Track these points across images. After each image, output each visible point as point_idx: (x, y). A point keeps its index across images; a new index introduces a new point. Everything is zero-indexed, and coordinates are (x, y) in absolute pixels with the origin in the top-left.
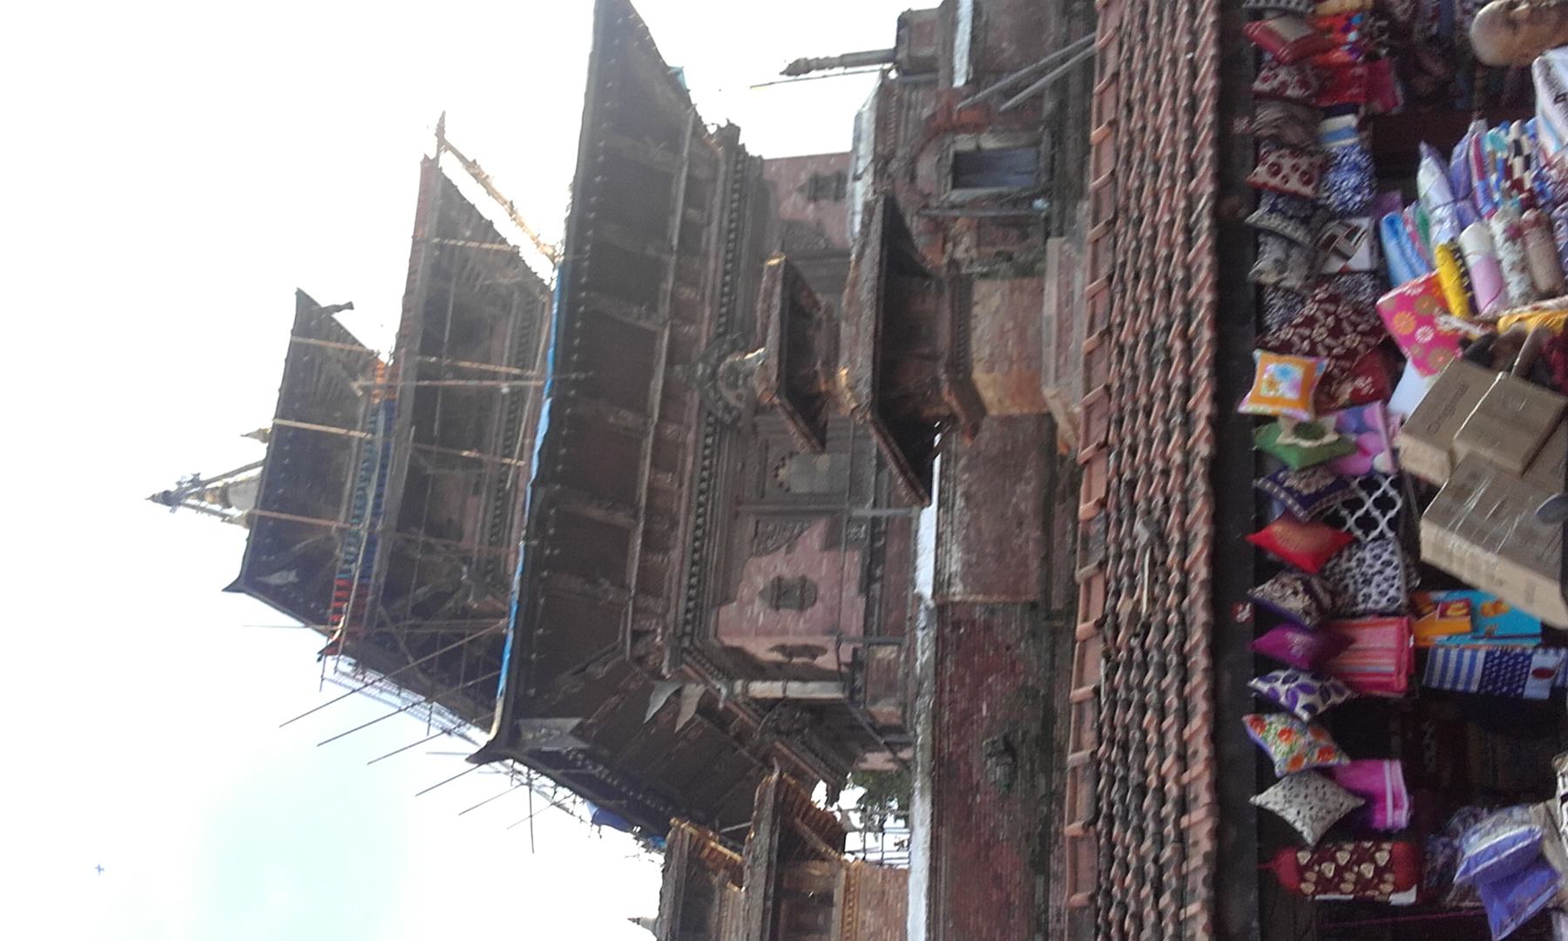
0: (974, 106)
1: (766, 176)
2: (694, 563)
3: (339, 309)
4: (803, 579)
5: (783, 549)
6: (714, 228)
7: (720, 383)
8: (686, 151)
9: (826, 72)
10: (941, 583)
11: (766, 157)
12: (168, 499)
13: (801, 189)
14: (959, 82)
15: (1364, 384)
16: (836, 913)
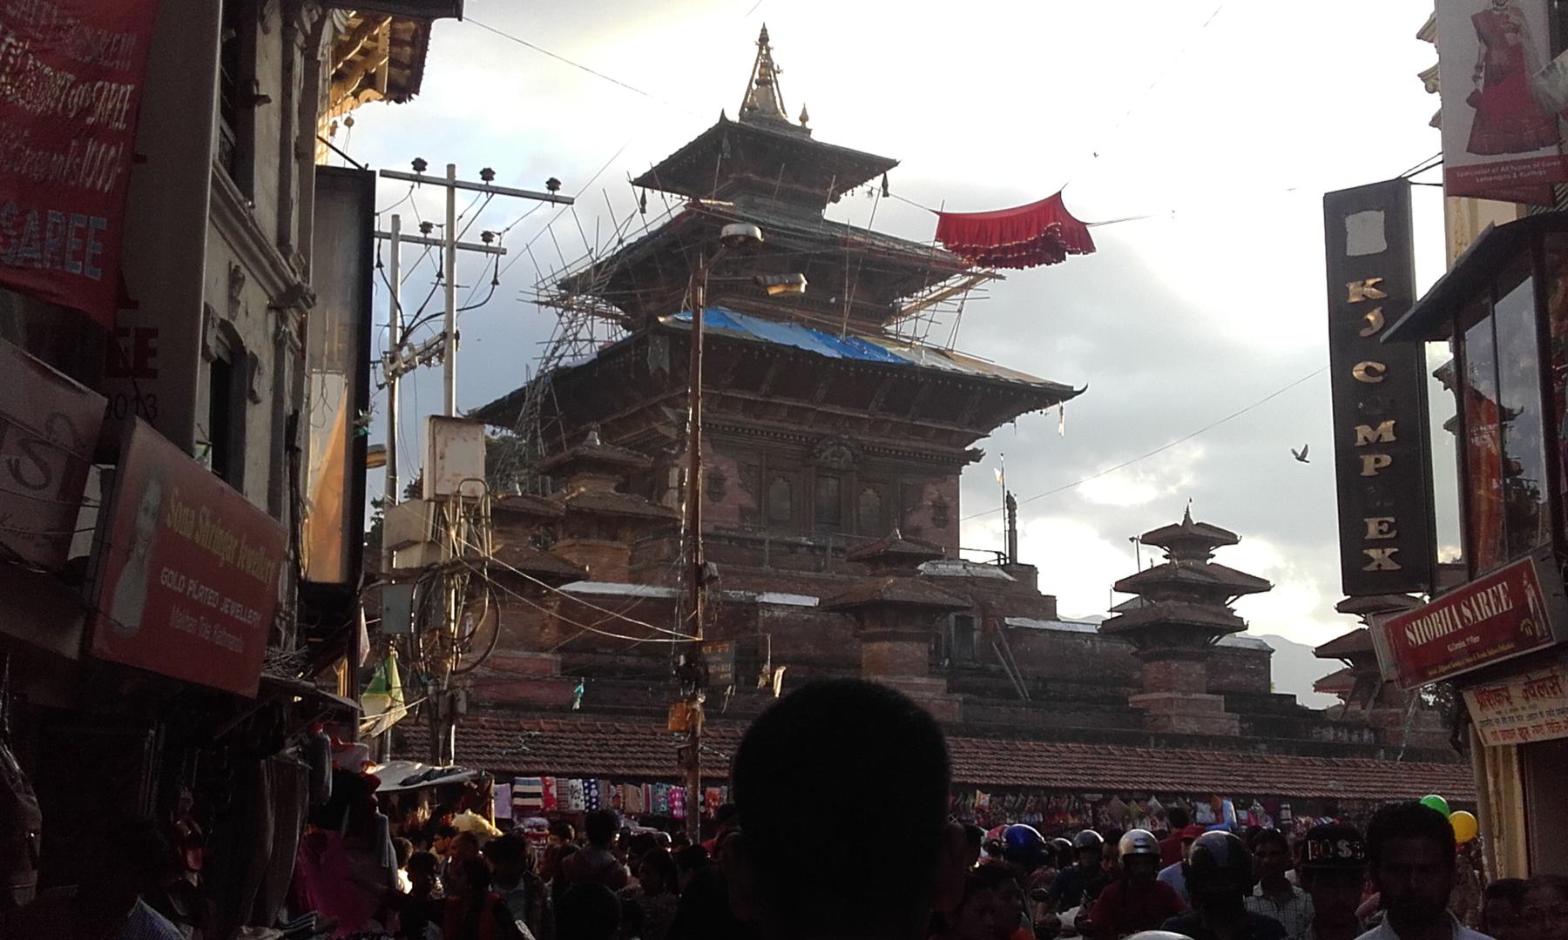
0: (995, 629)
1: (949, 477)
2: (736, 429)
3: (885, 185)
4: (724, 494)
5: (741, 482)
6: (923, 445)
7: (835, 448)
8: (968, 430)
9: (1007, 520)
10: (769, 606)
11: (961, 476)
12: (764, 39)
13: (940, 497)
14: (1007, 621)
15: (981, 820)
16: (608, 543)
